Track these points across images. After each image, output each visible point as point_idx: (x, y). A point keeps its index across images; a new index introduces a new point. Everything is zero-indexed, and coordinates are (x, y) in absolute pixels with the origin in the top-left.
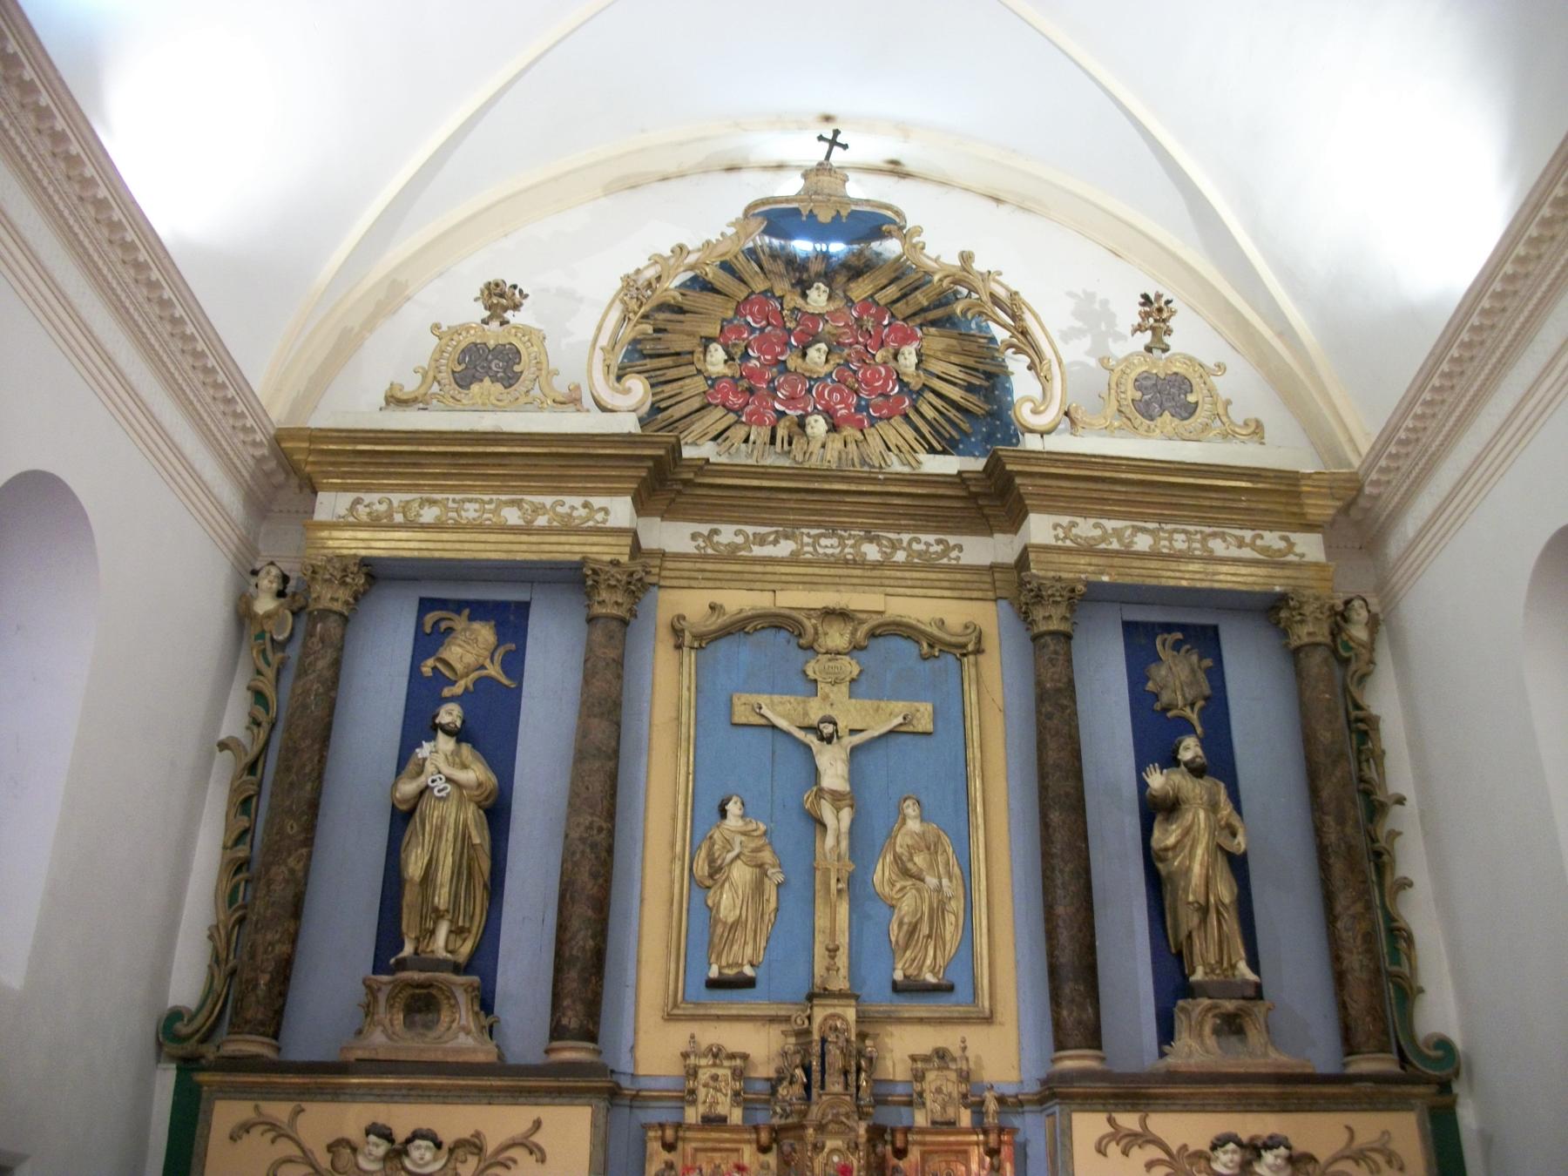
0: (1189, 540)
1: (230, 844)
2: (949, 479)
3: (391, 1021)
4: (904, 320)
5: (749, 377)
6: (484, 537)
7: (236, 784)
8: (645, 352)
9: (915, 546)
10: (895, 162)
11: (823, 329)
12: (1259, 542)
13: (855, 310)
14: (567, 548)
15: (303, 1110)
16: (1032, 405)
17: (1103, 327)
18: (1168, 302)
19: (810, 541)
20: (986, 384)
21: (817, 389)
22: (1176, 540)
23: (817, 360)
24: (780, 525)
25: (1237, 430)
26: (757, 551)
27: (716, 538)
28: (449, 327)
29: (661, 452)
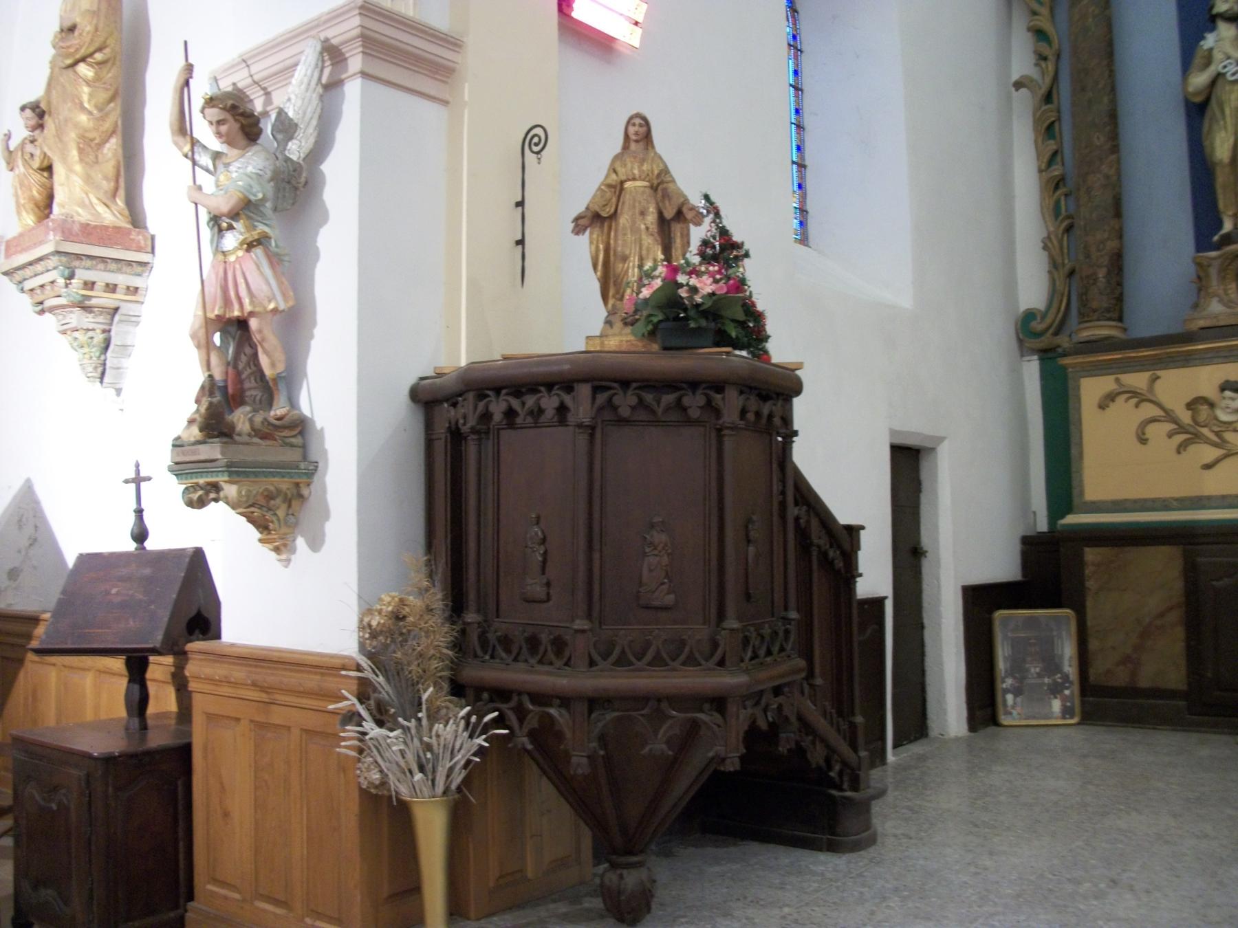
1: (1043, 167)
3: (1225, 291)
7: (1039, 114)
15: (1158, 378)
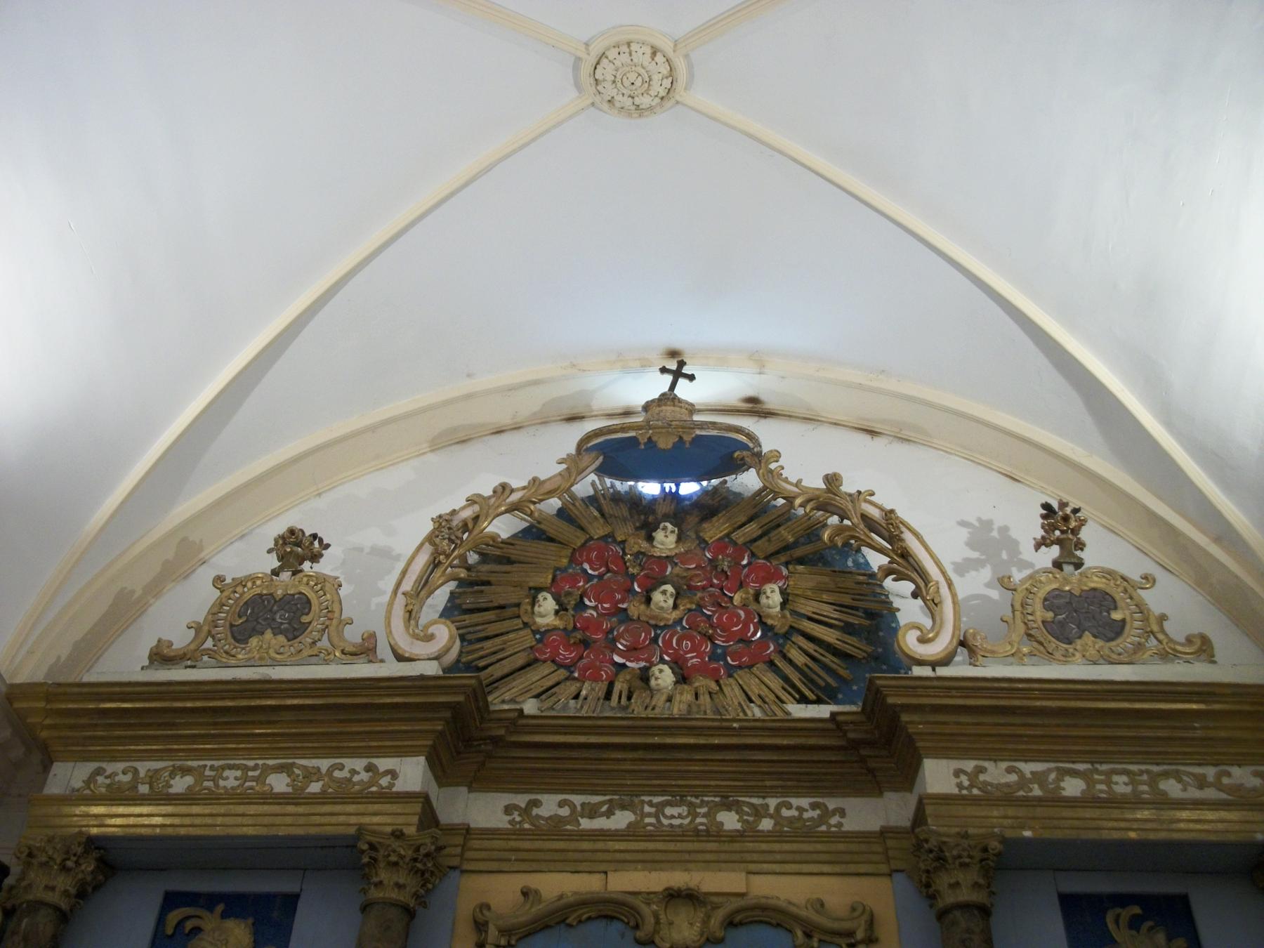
0: (1132, 782)
2: (820, 725)
4: (766, 558)
5: (584, 629)
6: (240, 809)
8: (464, 607)
9: (785, 813)
10: (753, 400)
11: (671, 573)
12: (1225, 780)
13: (709, 551)
14: (342, 819)
16: (918, 633)
17: (1004, 556)
18: (1076, 511)
19: (653, 810)
20: (867, 622)
21: (665, 635)
22: (1117, 783)
23: (663, 604)
24: (614, 793)
25: (1179, 648)
26: (585, 824)
27: (535, 811)
28: (233, 579)
29: (461, 698)
